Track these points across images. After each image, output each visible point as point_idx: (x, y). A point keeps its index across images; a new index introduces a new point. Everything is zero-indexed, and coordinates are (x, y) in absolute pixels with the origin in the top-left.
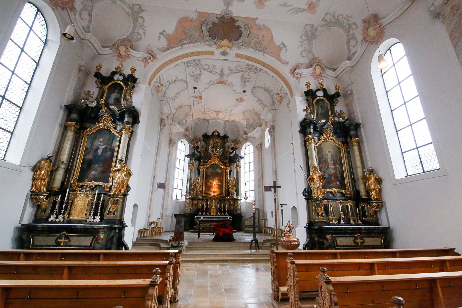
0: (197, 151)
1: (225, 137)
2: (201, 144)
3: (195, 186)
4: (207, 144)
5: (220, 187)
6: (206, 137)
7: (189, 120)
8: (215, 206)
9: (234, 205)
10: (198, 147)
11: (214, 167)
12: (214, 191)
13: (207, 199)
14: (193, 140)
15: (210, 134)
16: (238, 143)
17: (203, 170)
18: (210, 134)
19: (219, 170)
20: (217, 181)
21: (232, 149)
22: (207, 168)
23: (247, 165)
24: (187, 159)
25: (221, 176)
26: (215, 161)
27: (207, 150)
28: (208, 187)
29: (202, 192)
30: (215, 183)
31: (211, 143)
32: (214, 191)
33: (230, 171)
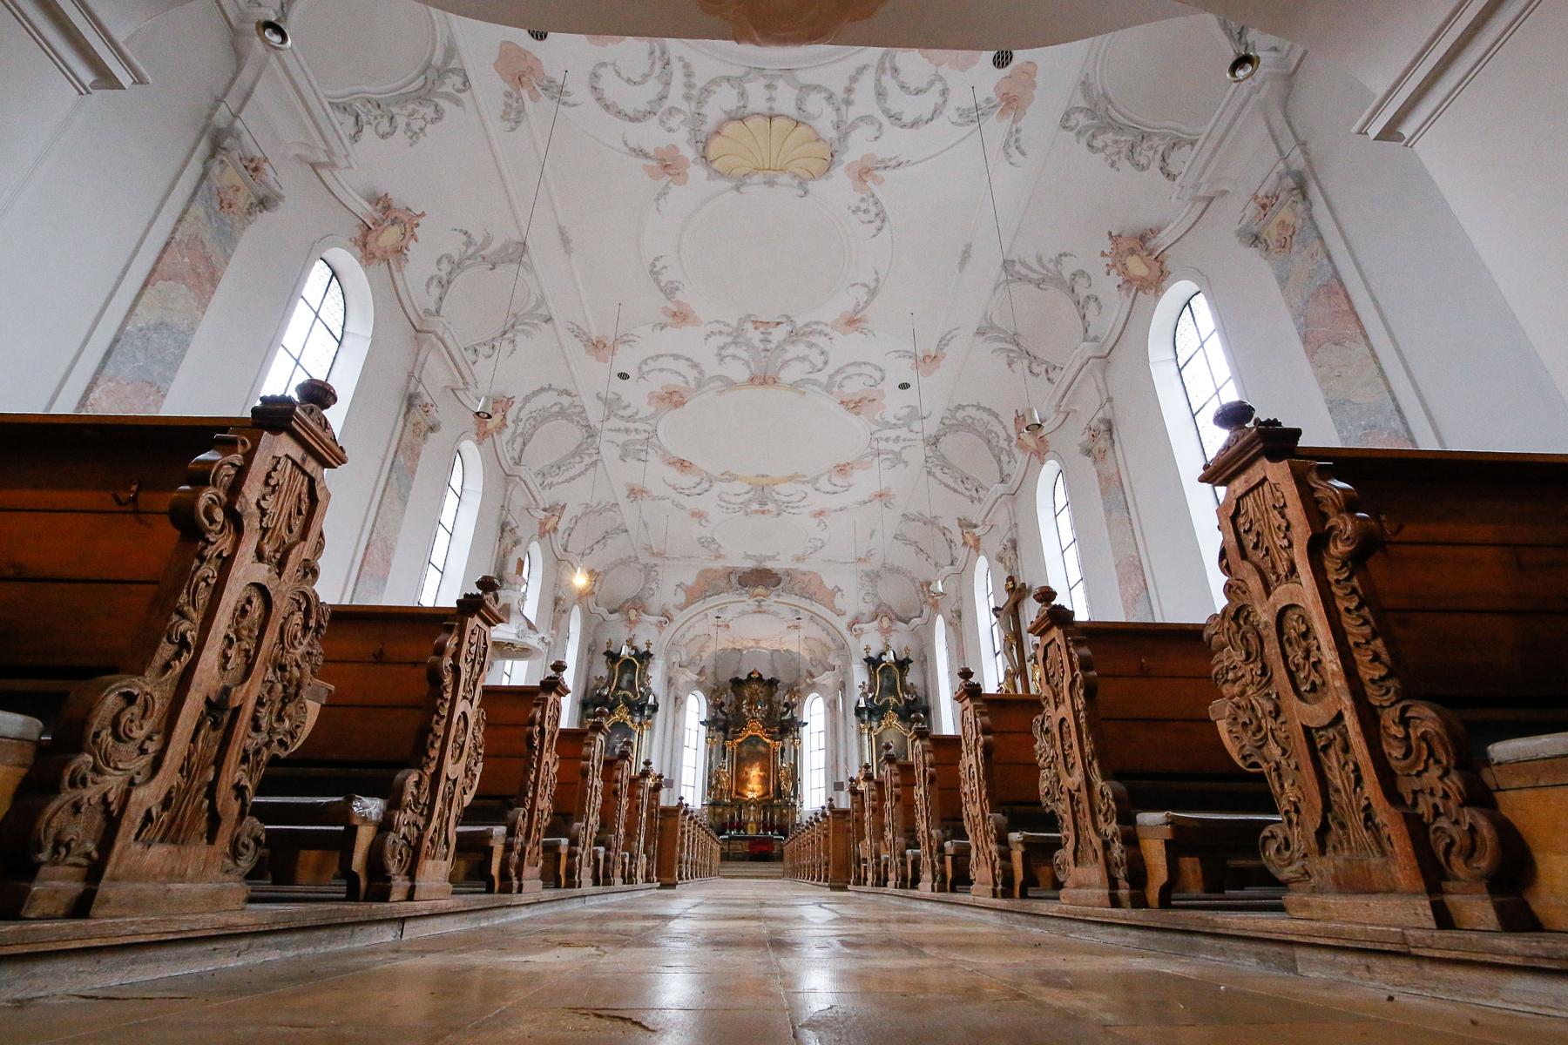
1: (772, 683)
2: (728, 698)
3: (718, 781)
4: (740, 697)
5: (765, 781)
6: (737, 683)
7: (705, 655)
10: (722, 704)
12: (754, 789)
13: (740, 803)
14: (714, 691)
15: (744, 677)
16: (795, 693)
18: (744, 677)
19: (762, 748)
21: (786, 705)
22: (740, 744)
23: (815, 737)
24: (703, 729)
25: (767, 760)
26: (754, 729)
27: (739, 708)
28: (742, 782)
29: (730, 791)
30: (755, 773)
32: (754, 789)
33: (783, 750)
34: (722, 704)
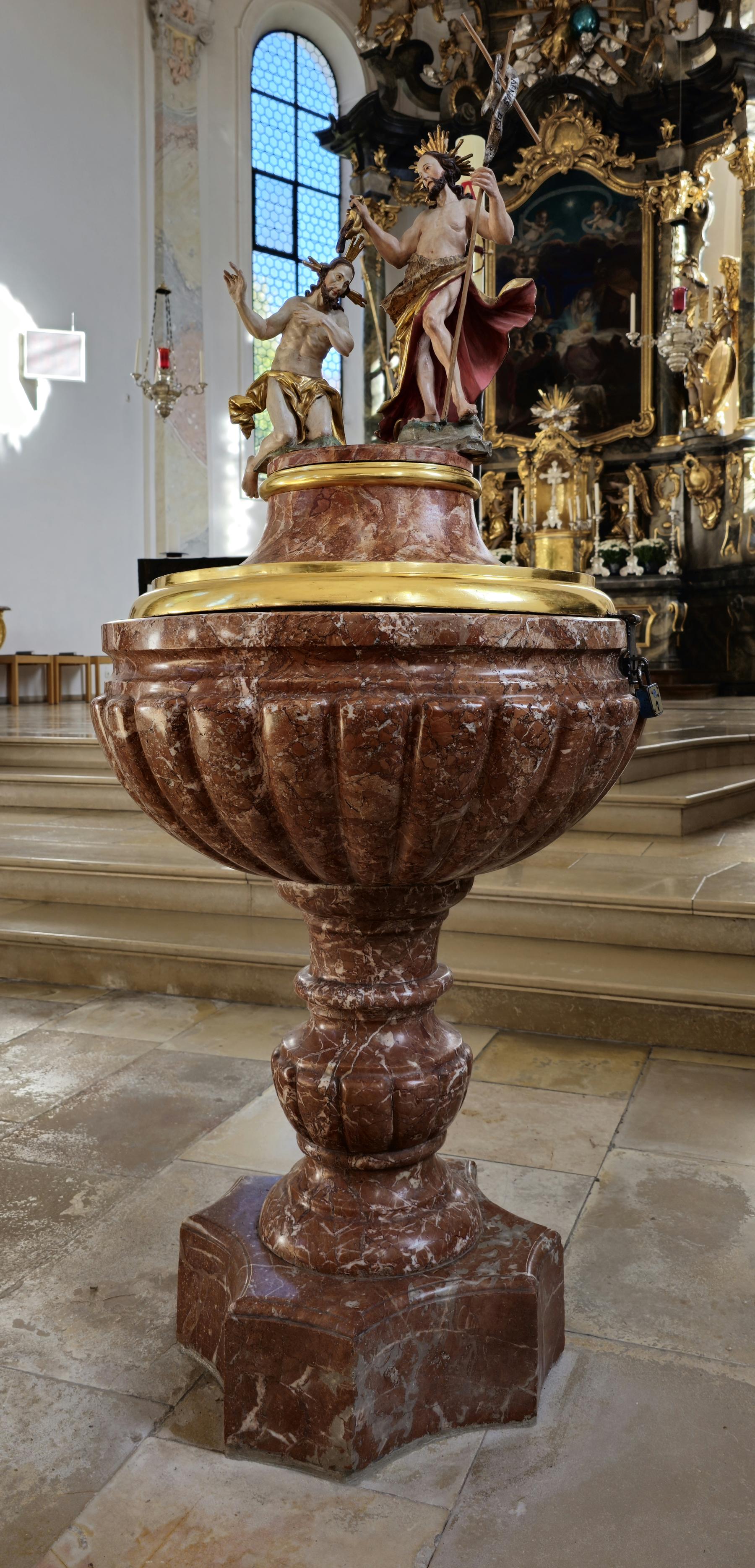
0: (419, 88)
8: (564, 517)
9: (721, 493)
11: (562, 198)
20: (588, 319)
34: (424, 54)
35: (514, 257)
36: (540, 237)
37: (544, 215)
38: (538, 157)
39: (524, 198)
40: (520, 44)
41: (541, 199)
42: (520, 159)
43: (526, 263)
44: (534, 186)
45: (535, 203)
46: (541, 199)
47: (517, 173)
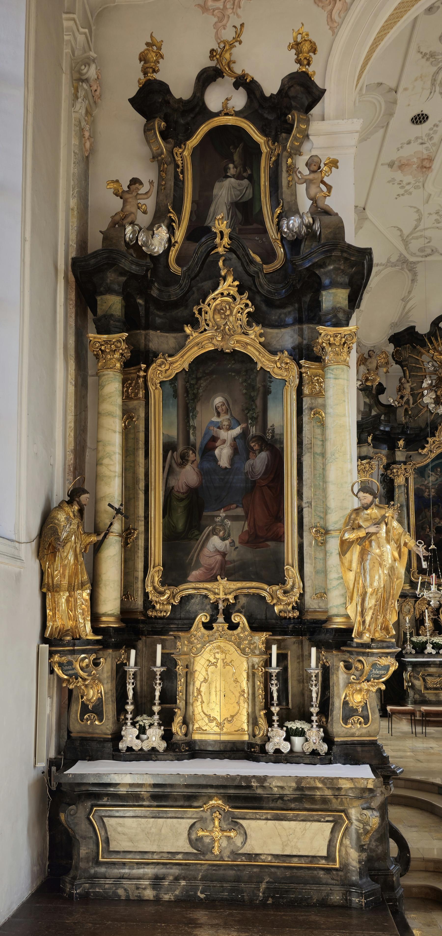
2: (390, 376)
17: (407, 480)
22: (421, 472)
31: (430, 367)
35: (424, 488)
36: (437, 480)
37: (439, 470)
38: (436, 443)
39: (429, 460)
40: (426, 389)
41: (437, 462)
42: (427, 442)
43: (429, 492)
44: (433, 456)
45: (434, 464)
46: (437, 462)
47: (426, 450)
